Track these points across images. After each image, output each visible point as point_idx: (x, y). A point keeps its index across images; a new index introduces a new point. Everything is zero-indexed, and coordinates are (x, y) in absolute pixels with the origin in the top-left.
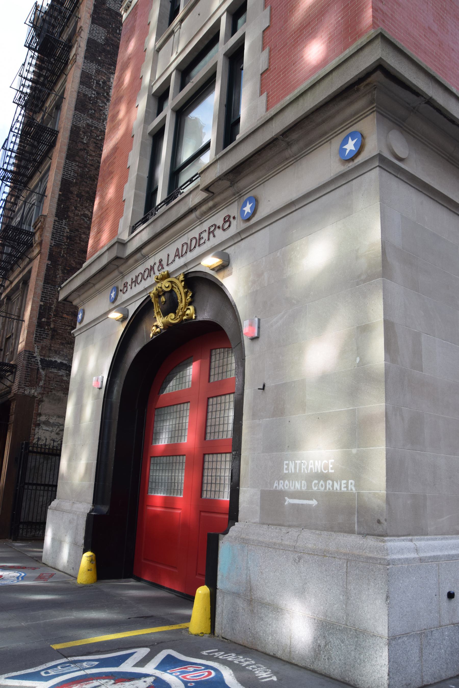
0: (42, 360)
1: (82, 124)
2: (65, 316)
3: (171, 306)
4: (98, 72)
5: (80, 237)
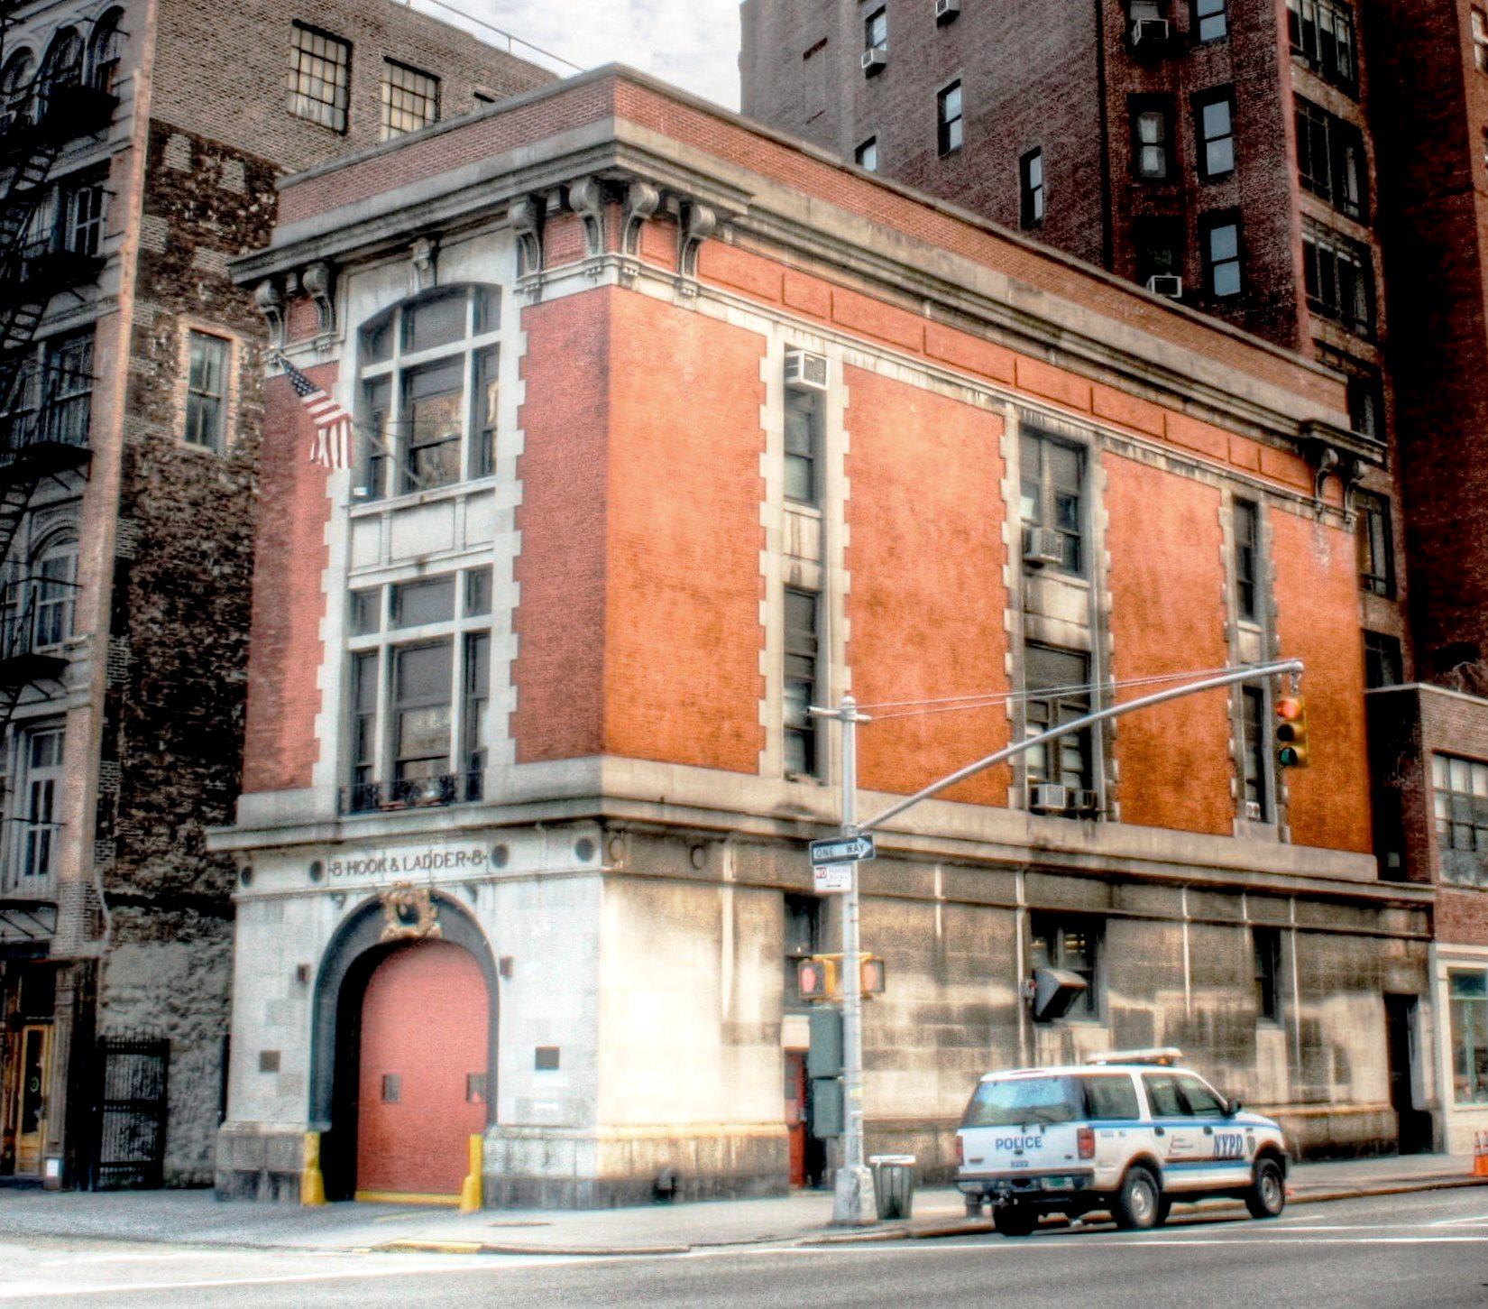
0: (108, 896)
1: (138, 439)
2: (134, 812)
3: (410, 917)
4: (159, 317)
5: (149, 665)
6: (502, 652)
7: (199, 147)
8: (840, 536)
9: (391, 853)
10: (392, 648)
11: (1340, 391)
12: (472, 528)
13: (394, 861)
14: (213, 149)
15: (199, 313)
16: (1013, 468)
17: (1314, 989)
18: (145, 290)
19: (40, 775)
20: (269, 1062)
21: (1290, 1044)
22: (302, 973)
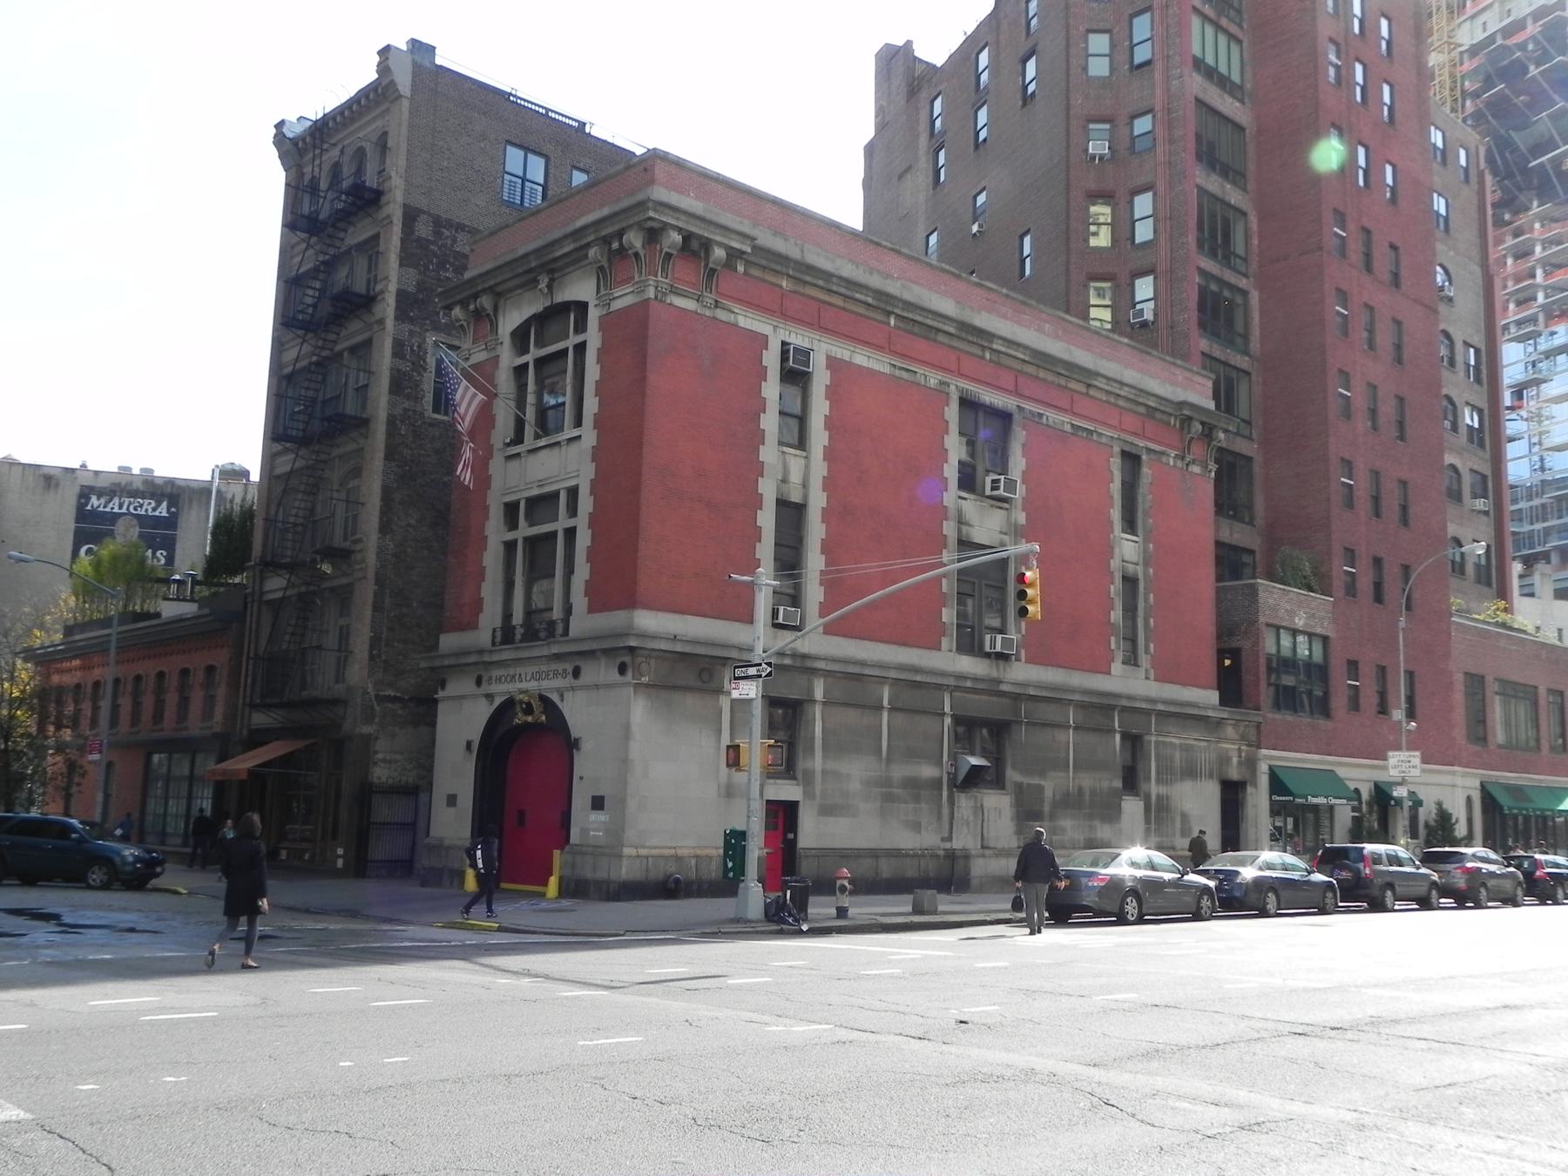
1: (398, 411)
4: (411, 333)
6: (583, 540)
7: (438, 223)
8: (819, 469)
10: (526, 539)
11: (1210, 384)
12: (568, 464)
14: (449, 224)
15: (441, 331)
16: (954, 427)
17: (1167, 774)
18: (401, 315)
19: (342, 622)
21: (1147, 809)
22: (469, 745)
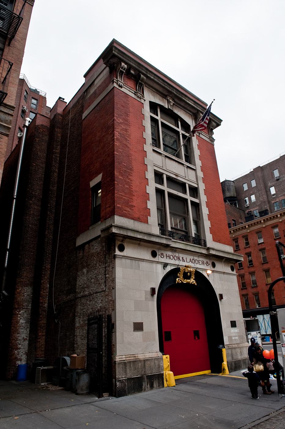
9: (181, 256)
13: (183, 258)
20: (138, 327)
